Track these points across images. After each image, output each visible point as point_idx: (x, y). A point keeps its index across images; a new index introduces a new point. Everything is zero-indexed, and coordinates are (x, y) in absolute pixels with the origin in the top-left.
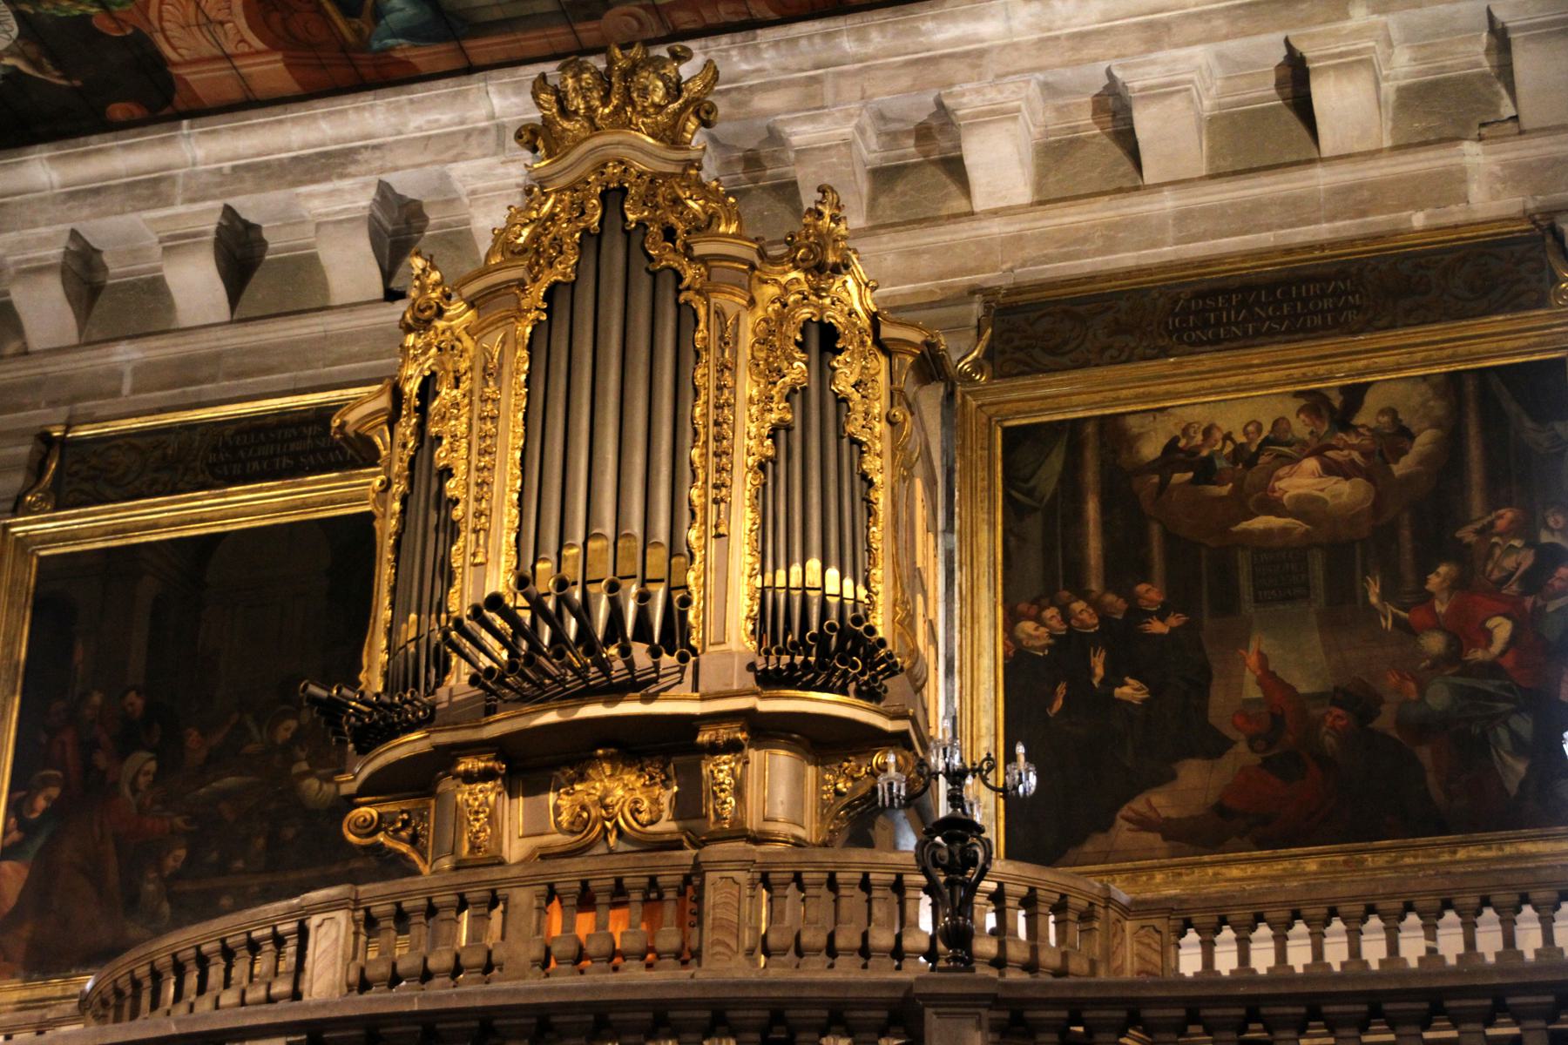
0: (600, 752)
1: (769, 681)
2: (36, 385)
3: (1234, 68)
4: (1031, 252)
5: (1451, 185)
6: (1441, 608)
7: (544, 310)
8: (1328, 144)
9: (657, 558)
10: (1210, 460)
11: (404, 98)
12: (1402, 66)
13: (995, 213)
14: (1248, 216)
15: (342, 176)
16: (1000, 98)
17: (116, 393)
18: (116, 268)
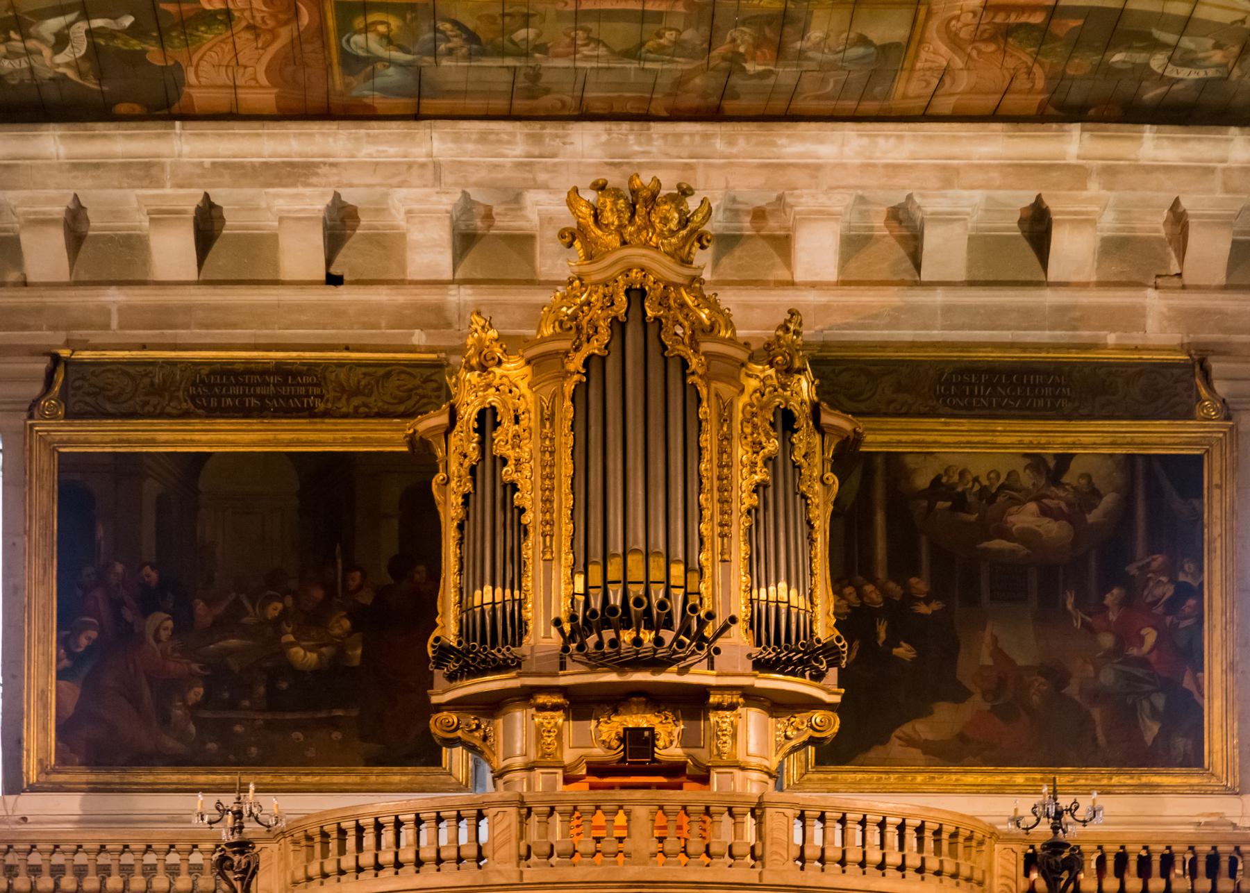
0: (635, 699)
1: (761, 666)
2: (38, 311)
3: (993, 207)
4: (837, 319)
5: (1134, 318)
6: (1113, 617)
7: (584, 374)
8: (1054, 273)
9: (677, 571)
10: (963, 494)
11: (362, 132)
12: (1108, 223)
13: (813, 285)
14: (994, 317)
15: (306, 185)
16: (829, 203)
17: (107, 327)
18: (97, 224)
